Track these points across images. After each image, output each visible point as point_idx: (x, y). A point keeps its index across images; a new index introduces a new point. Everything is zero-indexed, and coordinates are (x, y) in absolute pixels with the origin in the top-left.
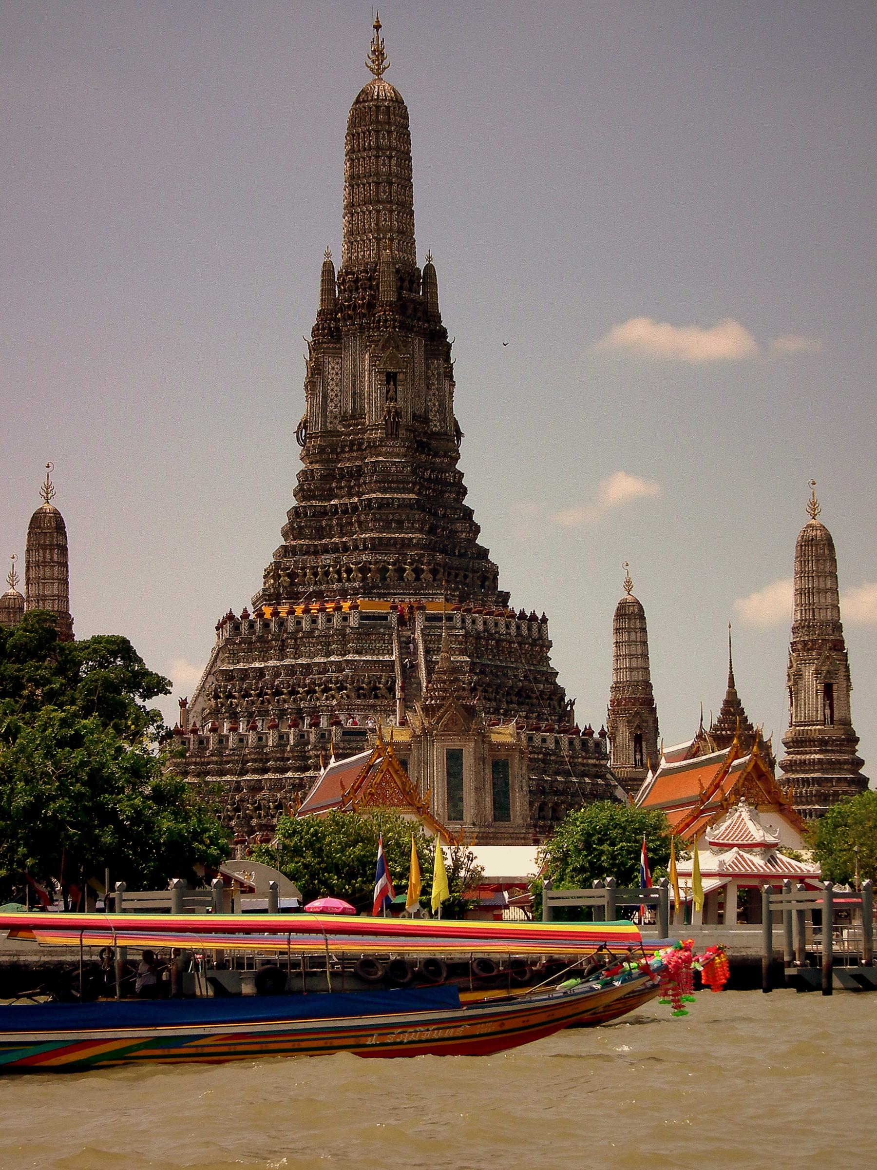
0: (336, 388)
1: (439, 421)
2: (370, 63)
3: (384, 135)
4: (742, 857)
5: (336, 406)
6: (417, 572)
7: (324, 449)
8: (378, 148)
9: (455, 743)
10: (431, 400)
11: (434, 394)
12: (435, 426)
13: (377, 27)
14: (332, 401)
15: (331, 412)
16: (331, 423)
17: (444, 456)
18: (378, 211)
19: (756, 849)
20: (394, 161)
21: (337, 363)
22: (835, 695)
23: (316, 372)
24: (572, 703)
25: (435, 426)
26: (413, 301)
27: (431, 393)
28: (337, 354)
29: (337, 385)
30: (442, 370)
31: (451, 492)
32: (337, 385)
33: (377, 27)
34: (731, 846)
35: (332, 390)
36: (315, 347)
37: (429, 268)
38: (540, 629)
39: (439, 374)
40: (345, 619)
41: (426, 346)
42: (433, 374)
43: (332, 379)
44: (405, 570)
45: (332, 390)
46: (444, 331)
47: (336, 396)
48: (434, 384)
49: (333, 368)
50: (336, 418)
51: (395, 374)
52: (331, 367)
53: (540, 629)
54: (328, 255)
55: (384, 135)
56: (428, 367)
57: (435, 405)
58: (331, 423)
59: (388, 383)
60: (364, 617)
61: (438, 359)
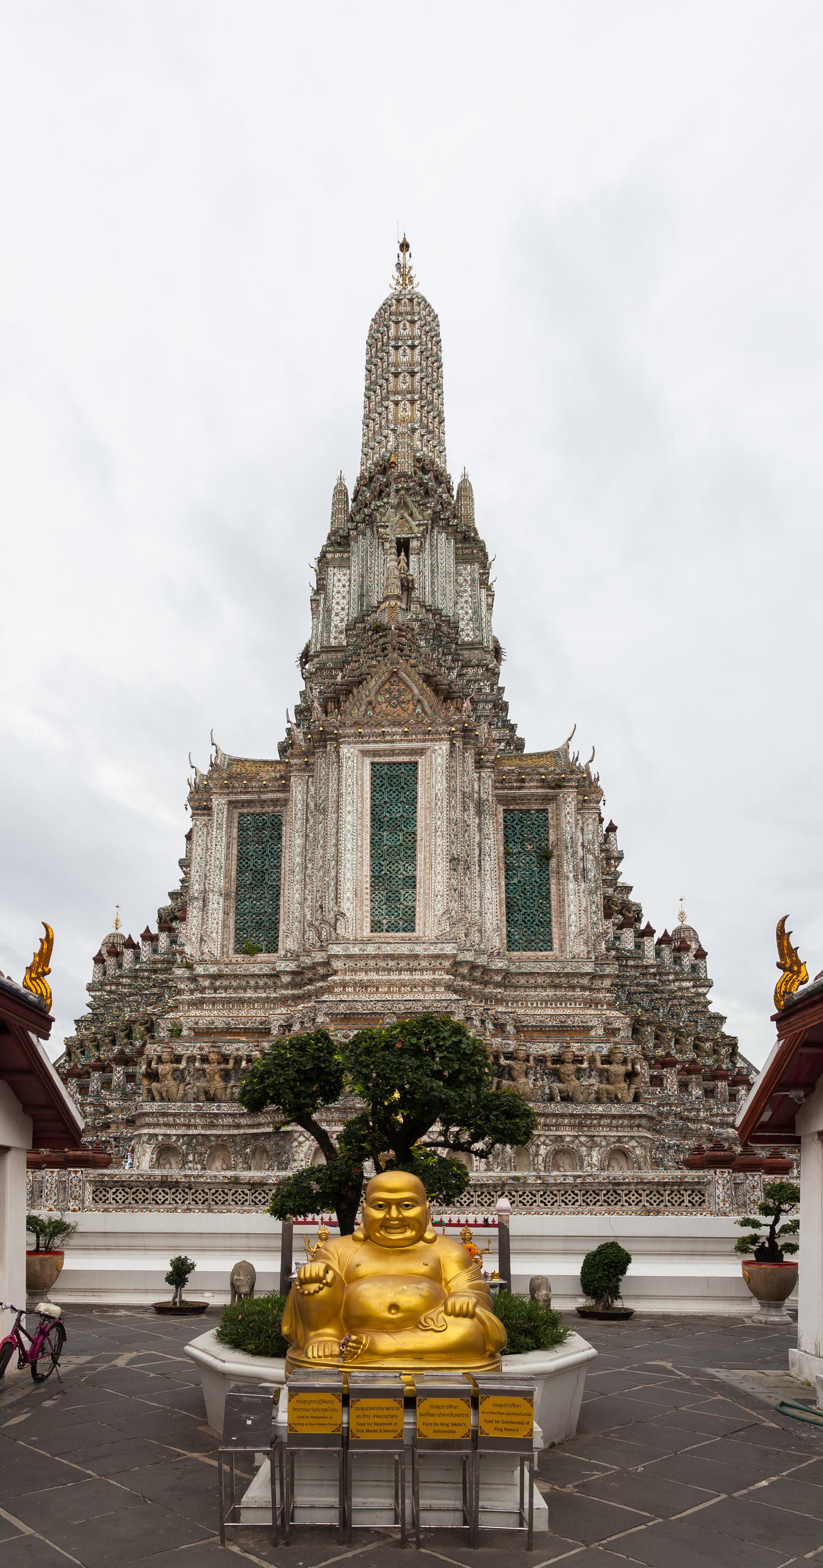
0: (342, 601)
1: (473, 630)
2: (394, 283)
3: (405, 325)
5: (342, 620)
7: (325, 664)
10: (462, 608)
11: (466, 602)
12: (468, 635)
13: (404, 246)
14: (337, 614)
15: (336, 626)
16: (335, 638)
17: (478, 666)
21: (345, 575)
23: (321, 587)
25: (467, 634)
27: (463, 600)
28: (344, 564)
29: (344, 597)
30: (477, 576)
31: (486, 702)
32: (344, 597)
35: (338, 603)
37: (465, 488)
39: (473, 580)
41: (457, 549)
42: (465, 580)
43: (338, 592)
45: (338, 603)
47: (343, 609)
48: (466, 591)
49: (339, 580)
50: (341, 632)
52: (337, 579)
55: (405, 325)
56: (458, 573)
57: (467, 613)
58: (335, 638)
61: (471, 563)
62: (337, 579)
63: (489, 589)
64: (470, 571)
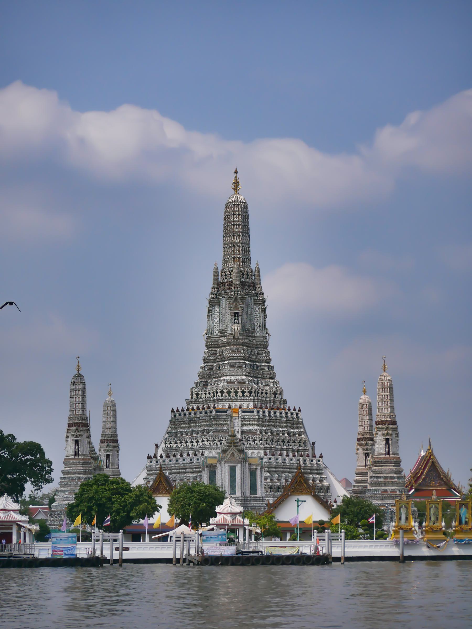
2: (233, 187)
4: (224, 518)
6: (243, 392)
8: (234, 221)
9: (233, 464)
13: (236, 172)
18: (234, 247)
19: (229, 515)
20: (241, 227)
22: (390, 443)
23: (210, 311)
24: (314, 444)
26: (248, 282)
28: (218, 303)
33: (236, 172)
34: (222, 513)
36: (210, 302)
38: (297, 414)
40: (211, 412)
44: (238, 392)
46: (263, 294)
51: (238, 313)
52: (216, 309)
53: (297, 414)
54: (216, 264)
59: (235, 316)
60: (217, 411)
62: (216, 309)
63: (265, 312)
64: (258, 308)
